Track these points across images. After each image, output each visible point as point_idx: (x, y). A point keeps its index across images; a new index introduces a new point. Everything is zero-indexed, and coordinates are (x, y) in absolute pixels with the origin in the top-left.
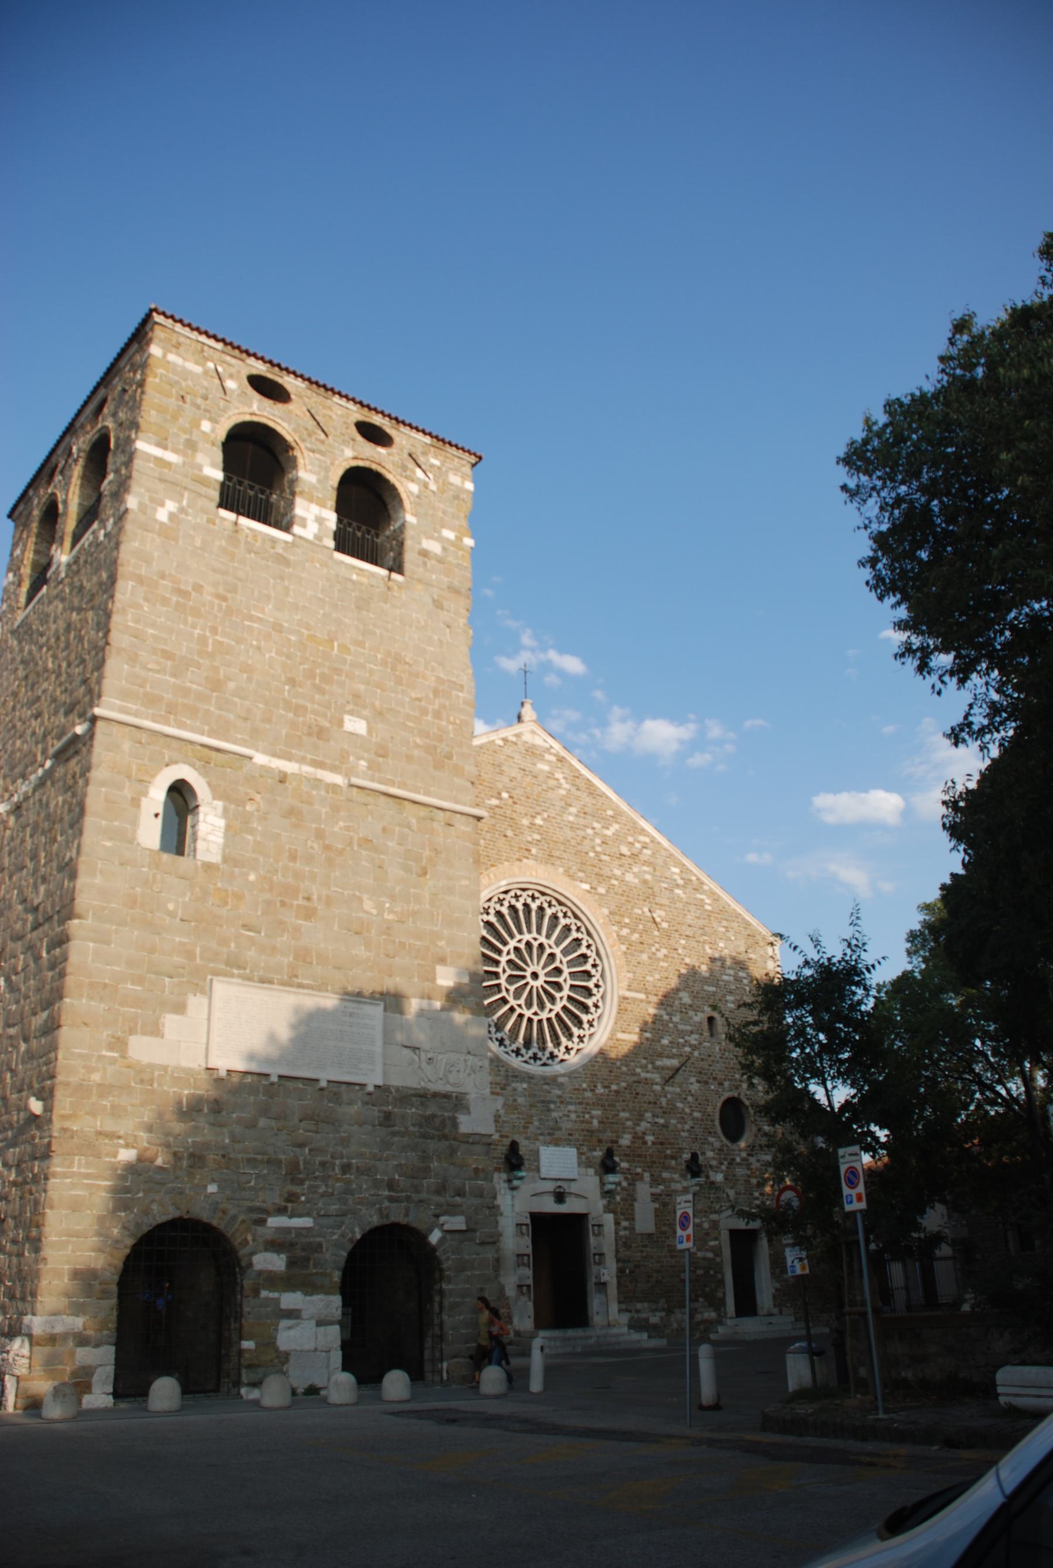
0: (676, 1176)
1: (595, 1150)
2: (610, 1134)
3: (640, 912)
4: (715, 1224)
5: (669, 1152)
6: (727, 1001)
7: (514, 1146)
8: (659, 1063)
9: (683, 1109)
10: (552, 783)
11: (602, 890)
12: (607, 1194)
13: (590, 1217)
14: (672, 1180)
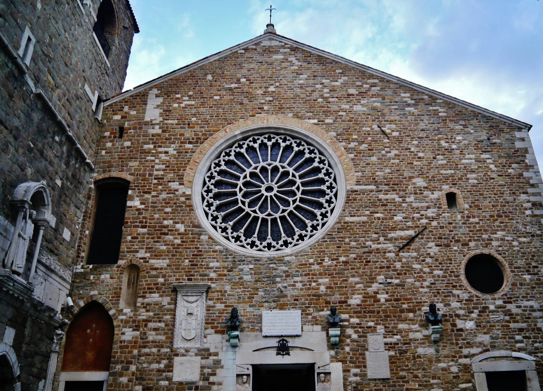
0: (416, 327)
1: (323, 310)
2: (339, 296)
3: (369, 129)
4: (466, 368)
5: (405, 306)
6: (468, 179)
7: (234, 315)
8: (392, 235)
9: (421, 270)
10: (284, 65)
11: (329, 121)
12: (332, 346)
13: (316, 367)
14: (411, 330)
